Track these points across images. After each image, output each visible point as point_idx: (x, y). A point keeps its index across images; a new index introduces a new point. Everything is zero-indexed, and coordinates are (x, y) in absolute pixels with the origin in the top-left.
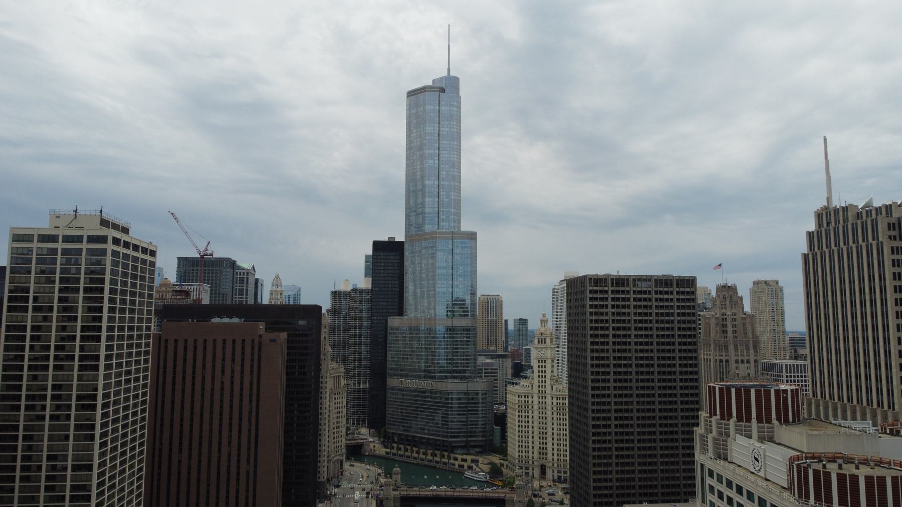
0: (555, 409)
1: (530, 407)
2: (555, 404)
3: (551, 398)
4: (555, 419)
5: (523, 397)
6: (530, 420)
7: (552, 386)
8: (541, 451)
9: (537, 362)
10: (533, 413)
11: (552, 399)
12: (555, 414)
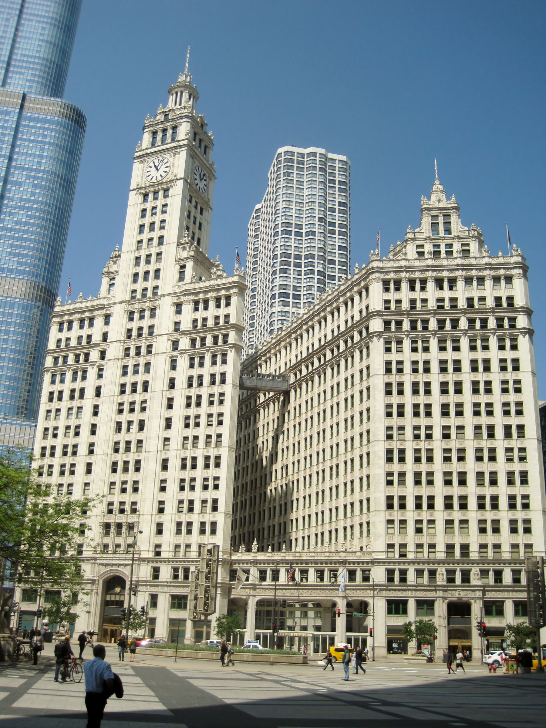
0: (184, 343)
1: (94, 355)
2: (186, 325)
3: (174, 309)
4: (181, 382)
5: (76, 325)
6: (88, 403)
7: (183, 267)
8: (112, 519)
9: (141, 197)
10: (100, 376)
11: (179, 312)
12: (183, 362)
